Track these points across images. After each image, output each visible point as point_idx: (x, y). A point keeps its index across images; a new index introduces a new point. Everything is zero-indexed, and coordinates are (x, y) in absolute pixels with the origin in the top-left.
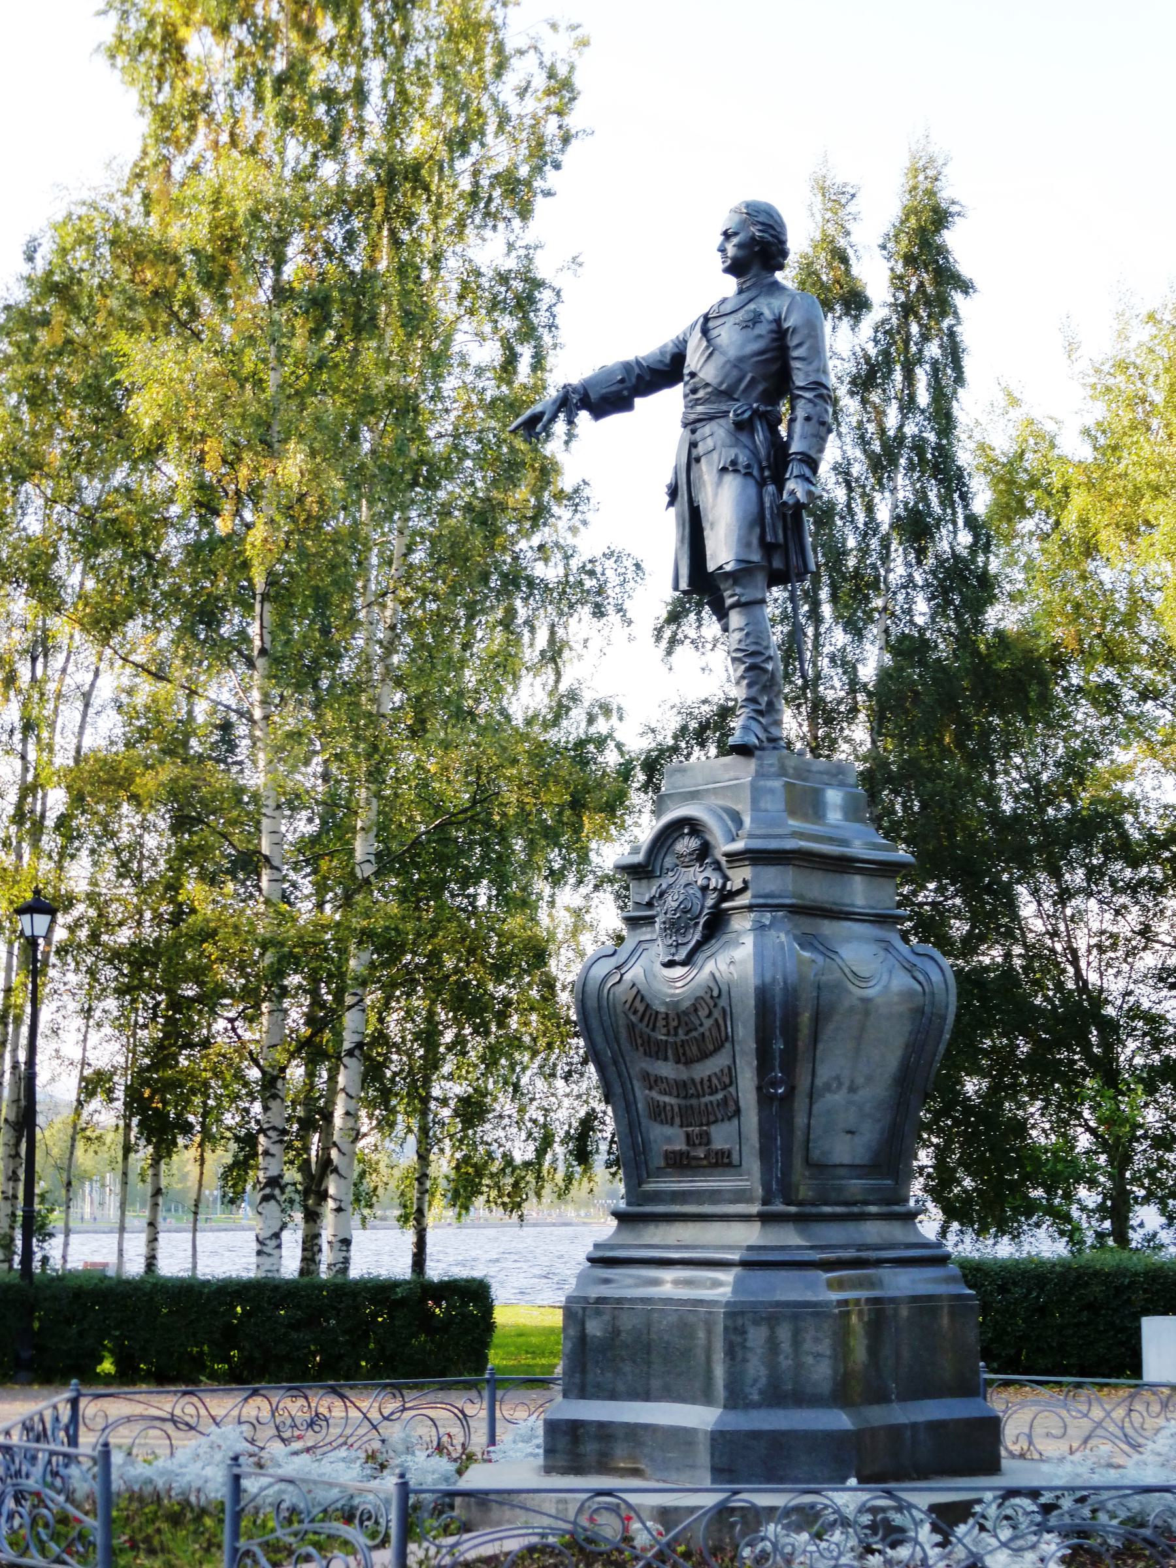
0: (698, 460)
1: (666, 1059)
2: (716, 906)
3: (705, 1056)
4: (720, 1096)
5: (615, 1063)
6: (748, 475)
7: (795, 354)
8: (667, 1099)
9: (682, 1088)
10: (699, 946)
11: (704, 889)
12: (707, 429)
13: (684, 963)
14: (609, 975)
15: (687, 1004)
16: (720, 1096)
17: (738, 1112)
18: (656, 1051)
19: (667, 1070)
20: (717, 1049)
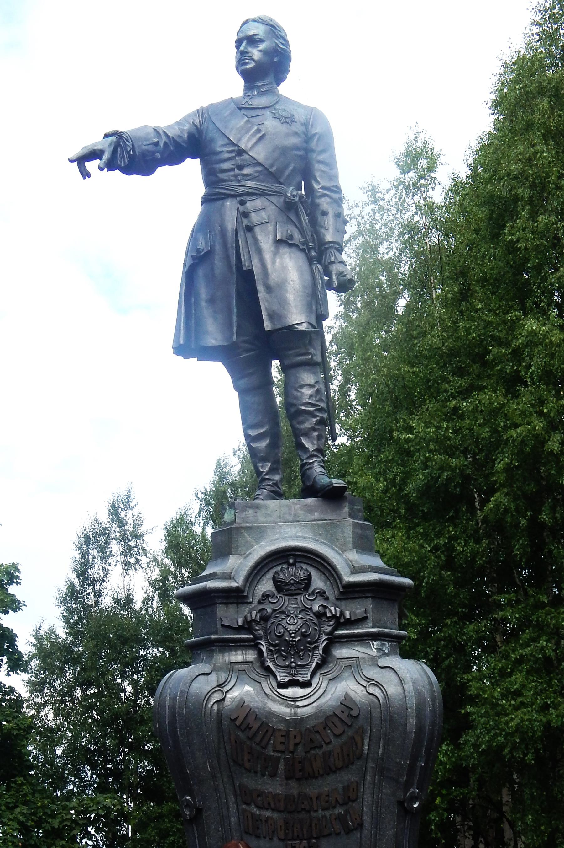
0: (250, 229)
1: (273, 775)
2: (331, 633)
3: (331, 770)
4: (340, 810)
5: (214, 777)
6: (303, 250)
7: (321, 158)
8: (268, 814)
9: (289, 805)
10: (319, 667)
11: (320, 615)
12: (259, 202)
13: (306, 684)
14: (212, 692)
15: (311, 723)
16: (340, 810)
17: (360, 826)
18: (268, 768)
19: (275, 787)
20: (346, 766)
